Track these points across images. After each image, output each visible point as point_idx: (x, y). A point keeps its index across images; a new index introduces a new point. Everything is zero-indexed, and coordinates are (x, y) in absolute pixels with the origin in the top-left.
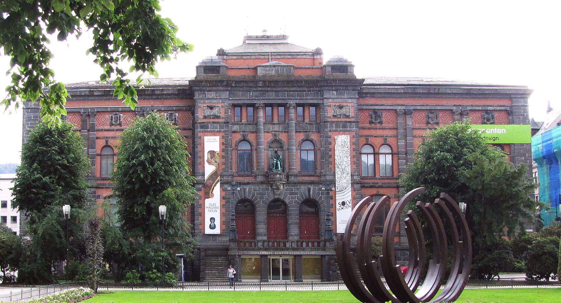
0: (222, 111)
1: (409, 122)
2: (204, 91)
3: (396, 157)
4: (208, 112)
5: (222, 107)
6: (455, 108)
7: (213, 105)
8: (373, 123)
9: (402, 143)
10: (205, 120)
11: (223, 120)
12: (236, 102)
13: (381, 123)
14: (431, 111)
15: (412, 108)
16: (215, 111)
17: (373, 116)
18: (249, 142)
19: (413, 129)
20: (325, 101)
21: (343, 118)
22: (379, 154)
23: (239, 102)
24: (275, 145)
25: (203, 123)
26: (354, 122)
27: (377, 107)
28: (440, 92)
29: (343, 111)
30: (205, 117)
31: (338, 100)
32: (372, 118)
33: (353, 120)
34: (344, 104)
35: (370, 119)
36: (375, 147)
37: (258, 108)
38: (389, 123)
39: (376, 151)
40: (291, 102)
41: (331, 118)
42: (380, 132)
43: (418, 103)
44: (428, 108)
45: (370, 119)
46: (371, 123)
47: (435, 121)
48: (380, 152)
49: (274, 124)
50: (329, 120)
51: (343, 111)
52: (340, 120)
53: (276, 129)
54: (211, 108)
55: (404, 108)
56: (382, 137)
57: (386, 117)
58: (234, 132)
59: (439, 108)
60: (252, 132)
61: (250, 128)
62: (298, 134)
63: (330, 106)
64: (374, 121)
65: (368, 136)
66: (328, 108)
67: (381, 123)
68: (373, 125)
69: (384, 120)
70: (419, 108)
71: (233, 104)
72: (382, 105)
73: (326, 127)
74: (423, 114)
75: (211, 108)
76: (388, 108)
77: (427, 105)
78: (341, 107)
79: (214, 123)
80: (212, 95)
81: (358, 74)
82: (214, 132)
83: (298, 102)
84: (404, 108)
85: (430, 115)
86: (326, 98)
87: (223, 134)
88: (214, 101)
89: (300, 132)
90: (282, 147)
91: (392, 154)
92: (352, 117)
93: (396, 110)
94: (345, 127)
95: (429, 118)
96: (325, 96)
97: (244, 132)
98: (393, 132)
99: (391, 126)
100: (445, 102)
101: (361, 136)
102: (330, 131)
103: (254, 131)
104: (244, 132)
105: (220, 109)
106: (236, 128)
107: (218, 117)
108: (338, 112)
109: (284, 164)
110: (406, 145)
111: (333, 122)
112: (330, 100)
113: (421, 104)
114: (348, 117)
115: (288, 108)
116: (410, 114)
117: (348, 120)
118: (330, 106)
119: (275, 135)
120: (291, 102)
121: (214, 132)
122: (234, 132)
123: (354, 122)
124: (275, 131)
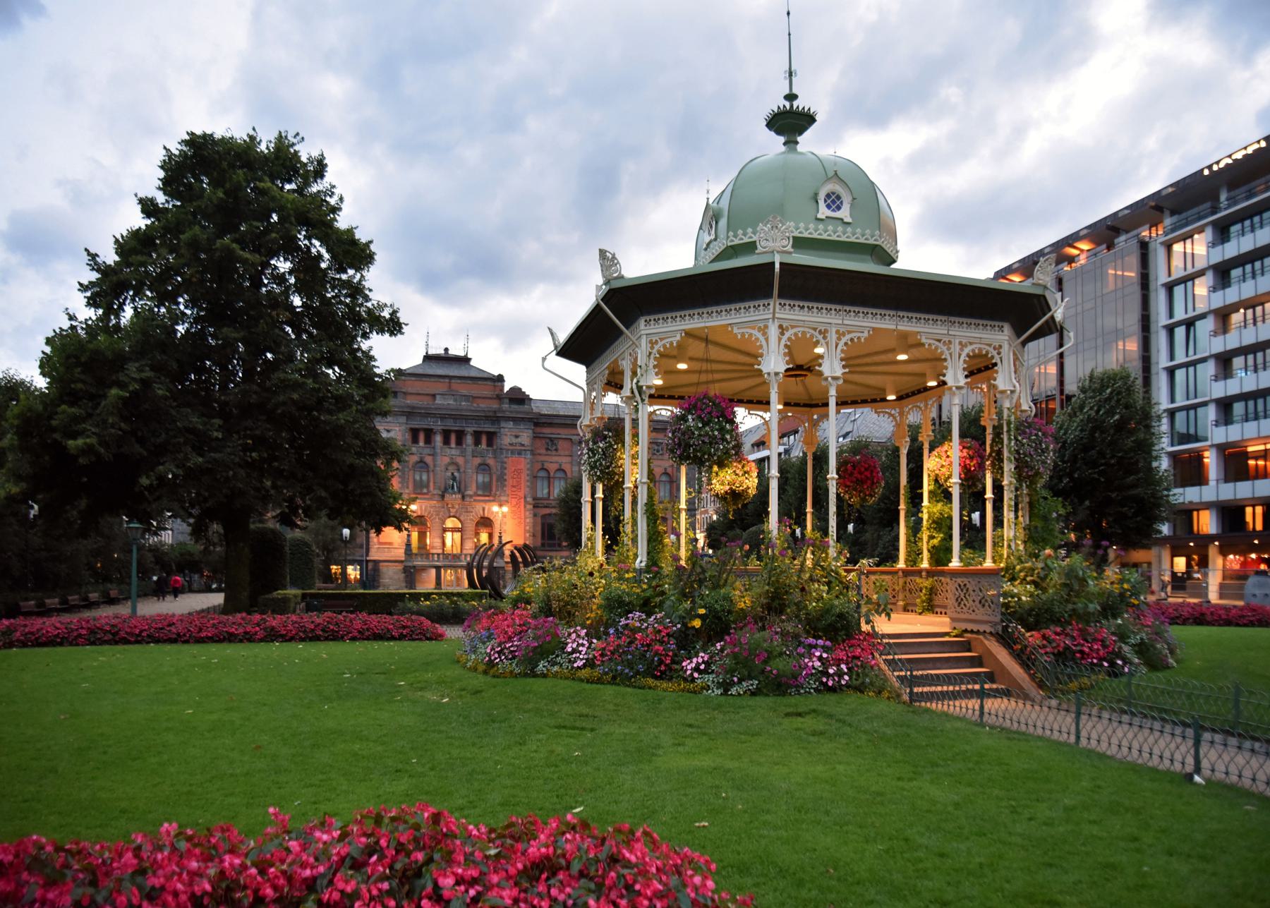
0: (399, 434)
13: (556, 450)
24: (450, 468)
29: (519, 440)
40: (469, 429)
42: (555, 459)
46: (547, 449)
51: (519, 440)
57: (561, 444)
67: (556, 450)
68: (549, 452)
73: (502, 453)
78: (517, 437)
90: (458, 470)
98: (568, 459)
99: (567, 453)
108: (514, 440)
114: (523, 445)
120: (469, 429)
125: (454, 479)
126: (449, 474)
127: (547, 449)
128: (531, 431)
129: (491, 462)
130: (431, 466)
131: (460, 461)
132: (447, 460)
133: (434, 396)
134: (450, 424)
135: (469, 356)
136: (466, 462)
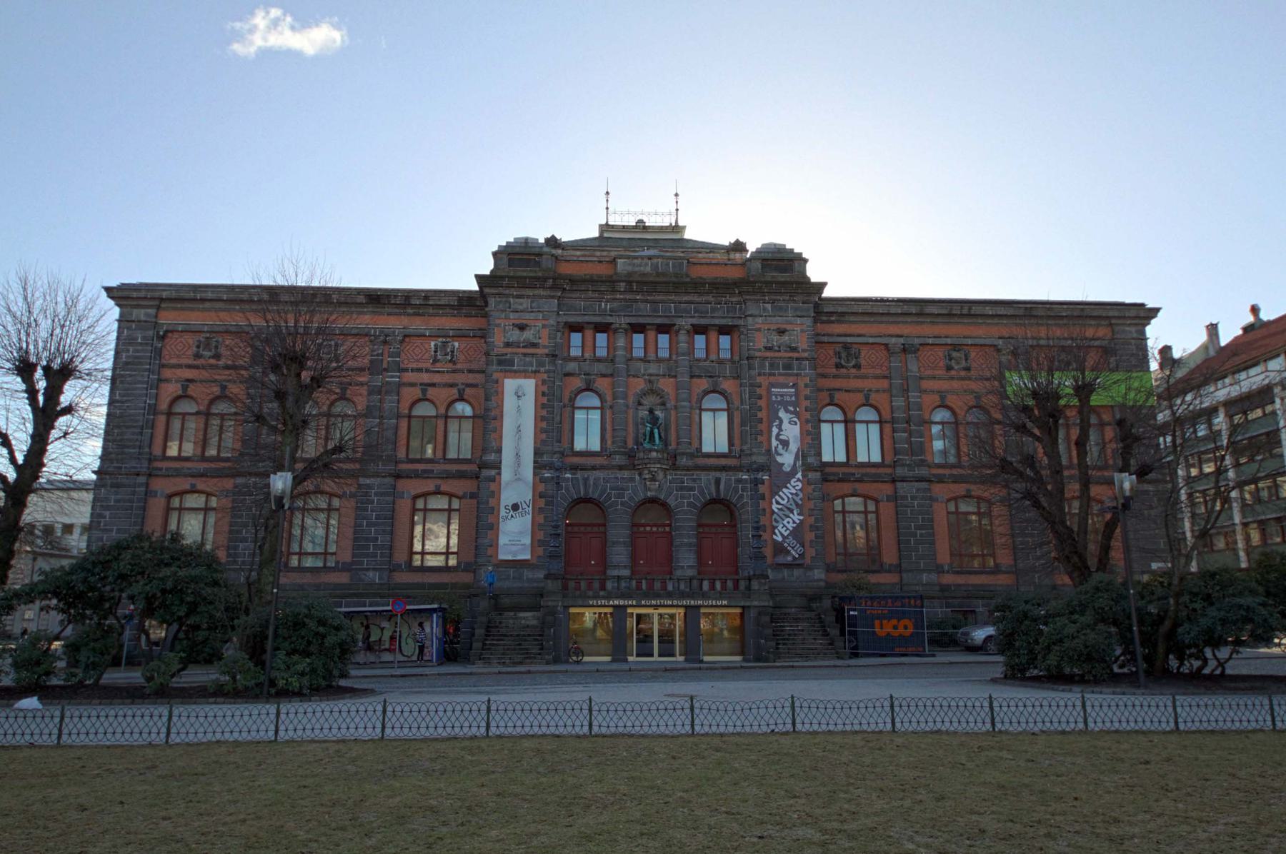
0: (545, 333)
1: (913, 367)
2: (508, 296)
3: (888, 428)
4: (515, 335)
5: (544, 326)
6: (1000, 342)
7: (524, 322)
8: (843, 367)
9: (899, 402)
10: (509, 350)
11: (546, 351)
12: (571, 320)
13: (857, 366)
14: (956, 347)
15: (917, 341)
16: (528, 335)
17: (844, 355)
18: (596, 392)
19: (921, 378)
20: (750, 319)
21: (786, 351)
22: (854, 421)
23: (580, 319)
24: (649, 401)
25: (503, 355)
26: (807, 359)
27: (849, 340)
28: (972, 312)
30: (508, 345)
31: (774, 320)
32: (840, 358)
33: (806, 355)
34: (788, 327)
35: (835, 360)
36: (847, 410)
37: (615, 331)
38: (873, 367)
39: (850, 416)
41: (760, 350)
43: (927, 331)
44: (949, 341)
45: (838, 360)
46: (838, 366)
47: (964, 364)
48: (858, 418)
49: (649, 362)
50: (758, 354)
51: (786, 338)
52: (777, 354)
53: (651, 371)
54: (522, 328)
55: (902, 340)
56: (859, 391)
58: (568, 375)
59: (970, 342)
60: (604, 376)
61: (601, 368)
62: (695, 380)
63: (759, 330)
64: (843, 362)
65: (834, 390)
66: (756, 334)
67: (857, 366)
68: (843, 371)
69: (863, 362)
70: (930, 341)
71: (566, 323)
72: (859, 336)
73: (750, 367)
74: (940, 353)
75: (522, 328)
76: (871, 340)
77: (946, 337)
79: (525, 355)
80: (525, 303)
81: (814, 273)
82: (525, 371)
83: (695, 321)
84: (902, 340)
85: (955, 354)
86: (751, 316)
87: (545, 376)
88: (527, 316)
89: (699, 377)
91: (881, 422)
92: (804, 351)
93: (886, 345)
94: (788, 367)
95: (950, 360)
96: (749, 313)
97: (588, 374)
100: (980, 331)
101: (820, 390)
102: (760, 375)
103: (609, 372)
104: (588, 374)
105: (541, 329)
106: (572, 367)
107: (534, 345)
108: (775, 340)
109: (666, 435)
110: (908, 407)
111: (766, 358)
112: (760, 320)
113: (936, 333)
114: (794, 349)
115: (677, 332)
116: (915, 352)
117: (795, 355)
118: (759, 330)
119: (650, 381)
121: (525, 371)
122: (568, 375)
123: (807, 359)
124: (651, 375)
125: (654, 421)
126: (643, 413)
127: (838, 366)
128: (808, 321)
129: (727, 385)
130: (609, 398)
131: (666, 385)
132: (639, 385)
133: (613, 261)
134: (644, 311)
135: (681, 224)
136: (677, 387)
